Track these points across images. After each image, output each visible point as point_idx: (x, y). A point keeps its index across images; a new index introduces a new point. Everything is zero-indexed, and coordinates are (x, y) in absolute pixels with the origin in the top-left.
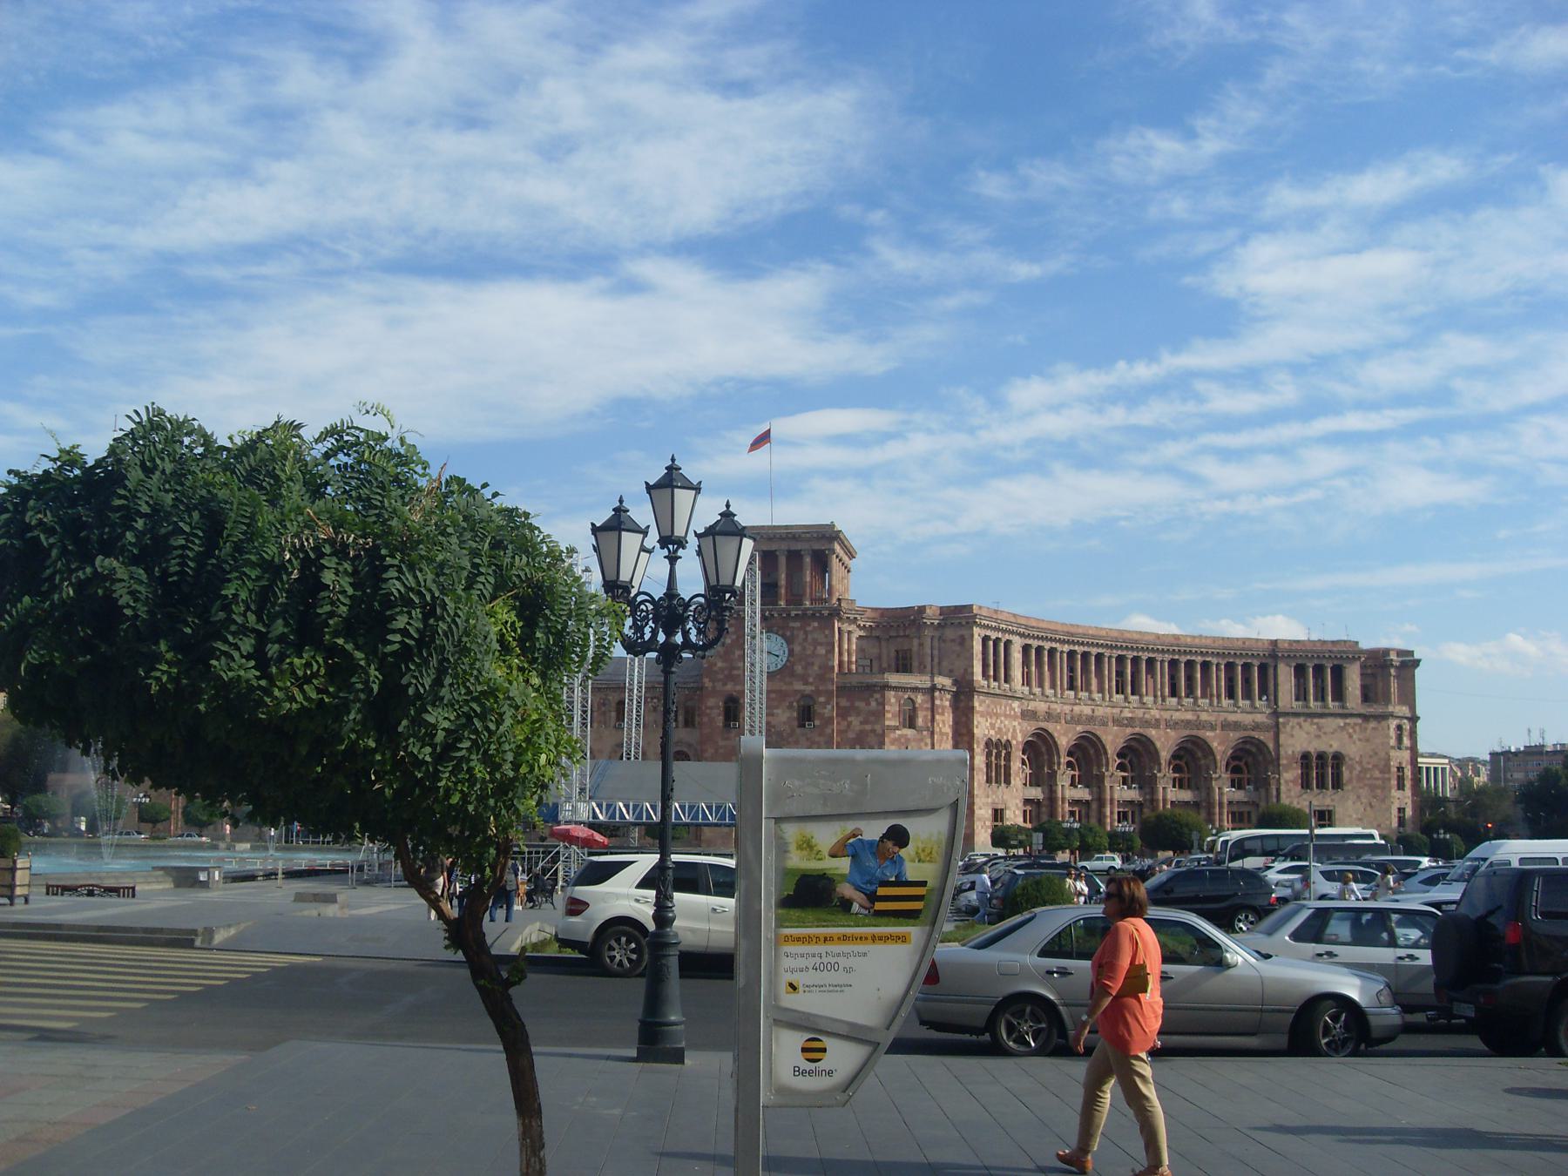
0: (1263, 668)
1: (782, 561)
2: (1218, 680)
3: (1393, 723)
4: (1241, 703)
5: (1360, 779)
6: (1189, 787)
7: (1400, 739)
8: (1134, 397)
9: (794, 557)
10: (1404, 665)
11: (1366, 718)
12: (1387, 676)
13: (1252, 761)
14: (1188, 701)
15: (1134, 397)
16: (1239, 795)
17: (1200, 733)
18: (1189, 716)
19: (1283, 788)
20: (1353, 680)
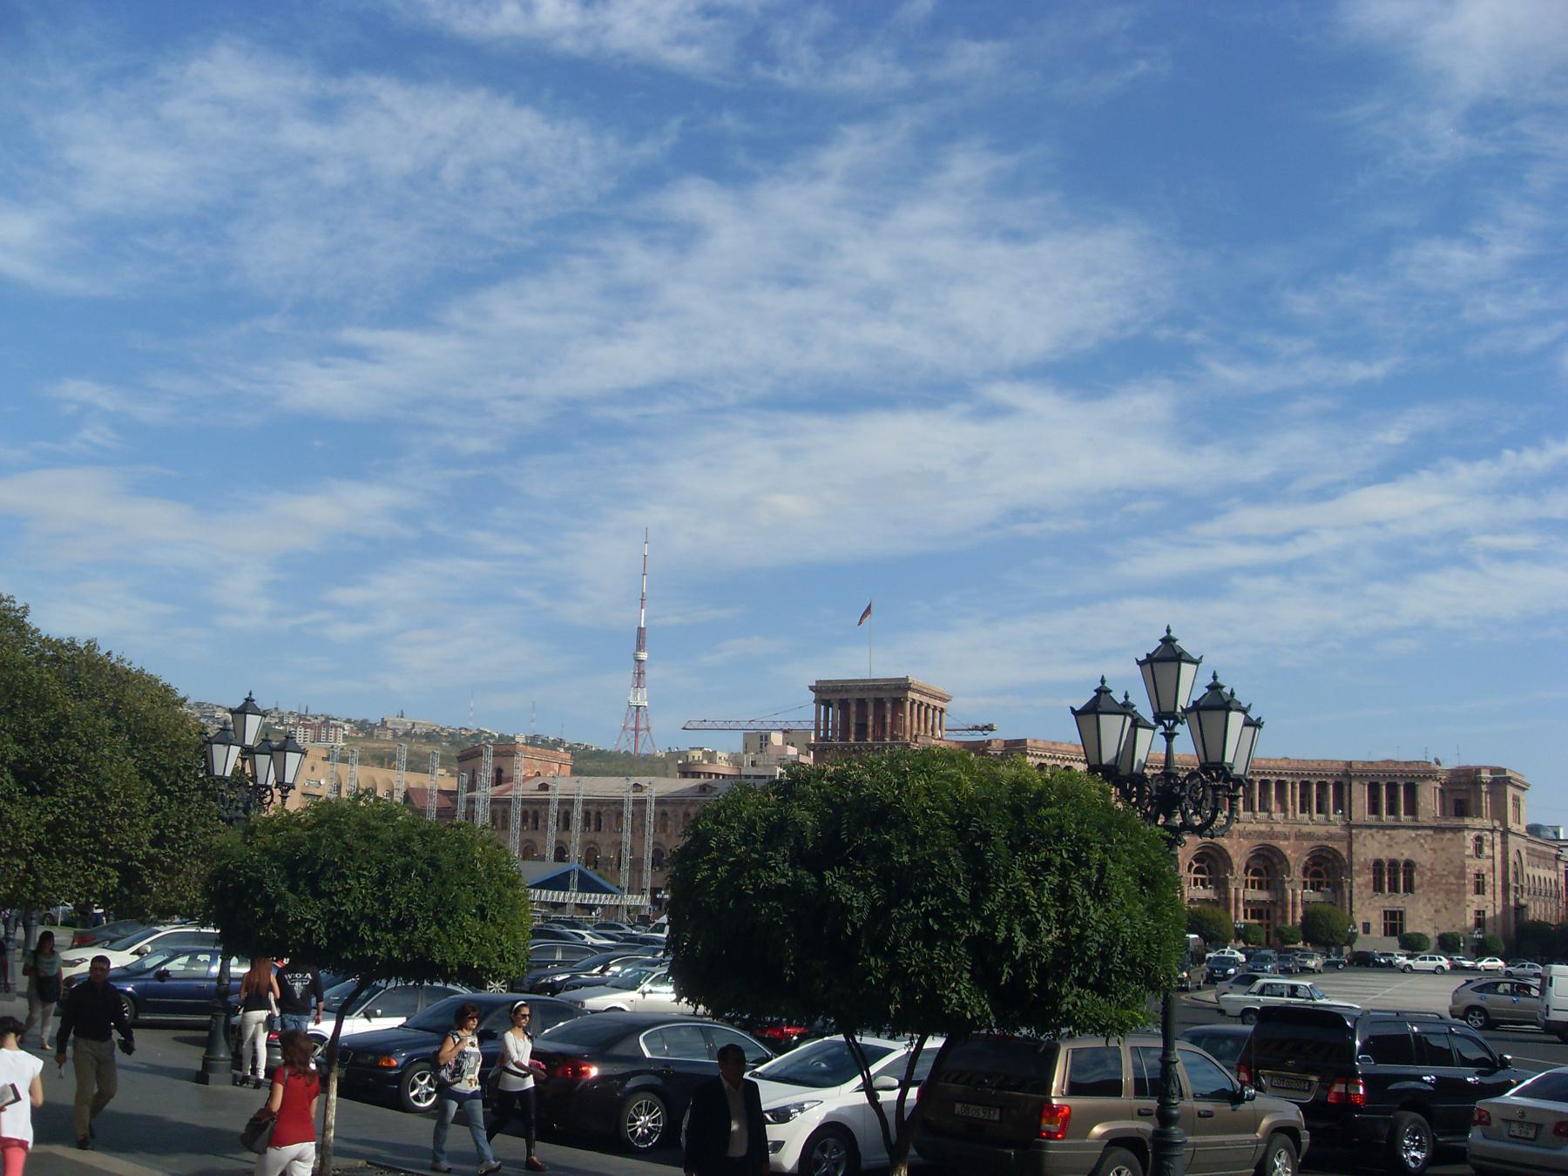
0: (1338, 787)
1: (871, 707)
2: (1293, 796)
3: (1470, 837)
4: (1315, 816)
5: (1431, 884)
6: (1268, 888)
7: (1479, 850)
8: (1536, 486)
9: (879, 703)
10: (1495, 782)
11: (1439, 829)
12: (1470, 793)
13: (1327, 867)
14: (1262, 815)
15: (1536, 486)
16: (1312, 895)
17: (1274, 843)
18: (1263, 828)
19: (1355, 891)
20: (1429, 799)
